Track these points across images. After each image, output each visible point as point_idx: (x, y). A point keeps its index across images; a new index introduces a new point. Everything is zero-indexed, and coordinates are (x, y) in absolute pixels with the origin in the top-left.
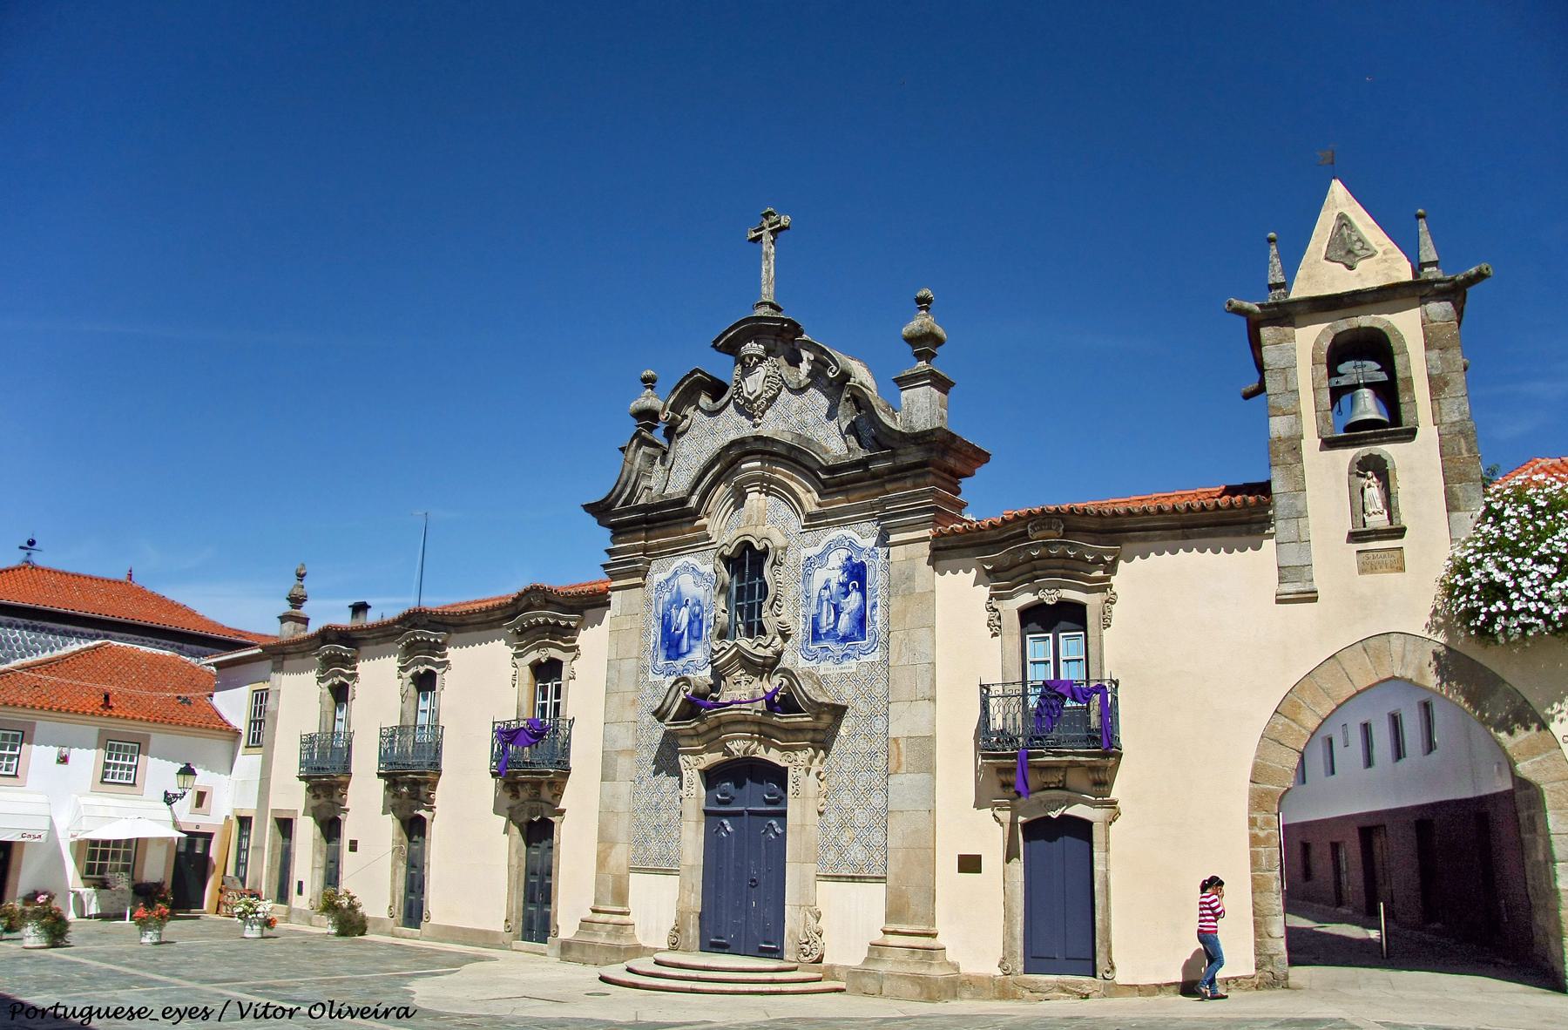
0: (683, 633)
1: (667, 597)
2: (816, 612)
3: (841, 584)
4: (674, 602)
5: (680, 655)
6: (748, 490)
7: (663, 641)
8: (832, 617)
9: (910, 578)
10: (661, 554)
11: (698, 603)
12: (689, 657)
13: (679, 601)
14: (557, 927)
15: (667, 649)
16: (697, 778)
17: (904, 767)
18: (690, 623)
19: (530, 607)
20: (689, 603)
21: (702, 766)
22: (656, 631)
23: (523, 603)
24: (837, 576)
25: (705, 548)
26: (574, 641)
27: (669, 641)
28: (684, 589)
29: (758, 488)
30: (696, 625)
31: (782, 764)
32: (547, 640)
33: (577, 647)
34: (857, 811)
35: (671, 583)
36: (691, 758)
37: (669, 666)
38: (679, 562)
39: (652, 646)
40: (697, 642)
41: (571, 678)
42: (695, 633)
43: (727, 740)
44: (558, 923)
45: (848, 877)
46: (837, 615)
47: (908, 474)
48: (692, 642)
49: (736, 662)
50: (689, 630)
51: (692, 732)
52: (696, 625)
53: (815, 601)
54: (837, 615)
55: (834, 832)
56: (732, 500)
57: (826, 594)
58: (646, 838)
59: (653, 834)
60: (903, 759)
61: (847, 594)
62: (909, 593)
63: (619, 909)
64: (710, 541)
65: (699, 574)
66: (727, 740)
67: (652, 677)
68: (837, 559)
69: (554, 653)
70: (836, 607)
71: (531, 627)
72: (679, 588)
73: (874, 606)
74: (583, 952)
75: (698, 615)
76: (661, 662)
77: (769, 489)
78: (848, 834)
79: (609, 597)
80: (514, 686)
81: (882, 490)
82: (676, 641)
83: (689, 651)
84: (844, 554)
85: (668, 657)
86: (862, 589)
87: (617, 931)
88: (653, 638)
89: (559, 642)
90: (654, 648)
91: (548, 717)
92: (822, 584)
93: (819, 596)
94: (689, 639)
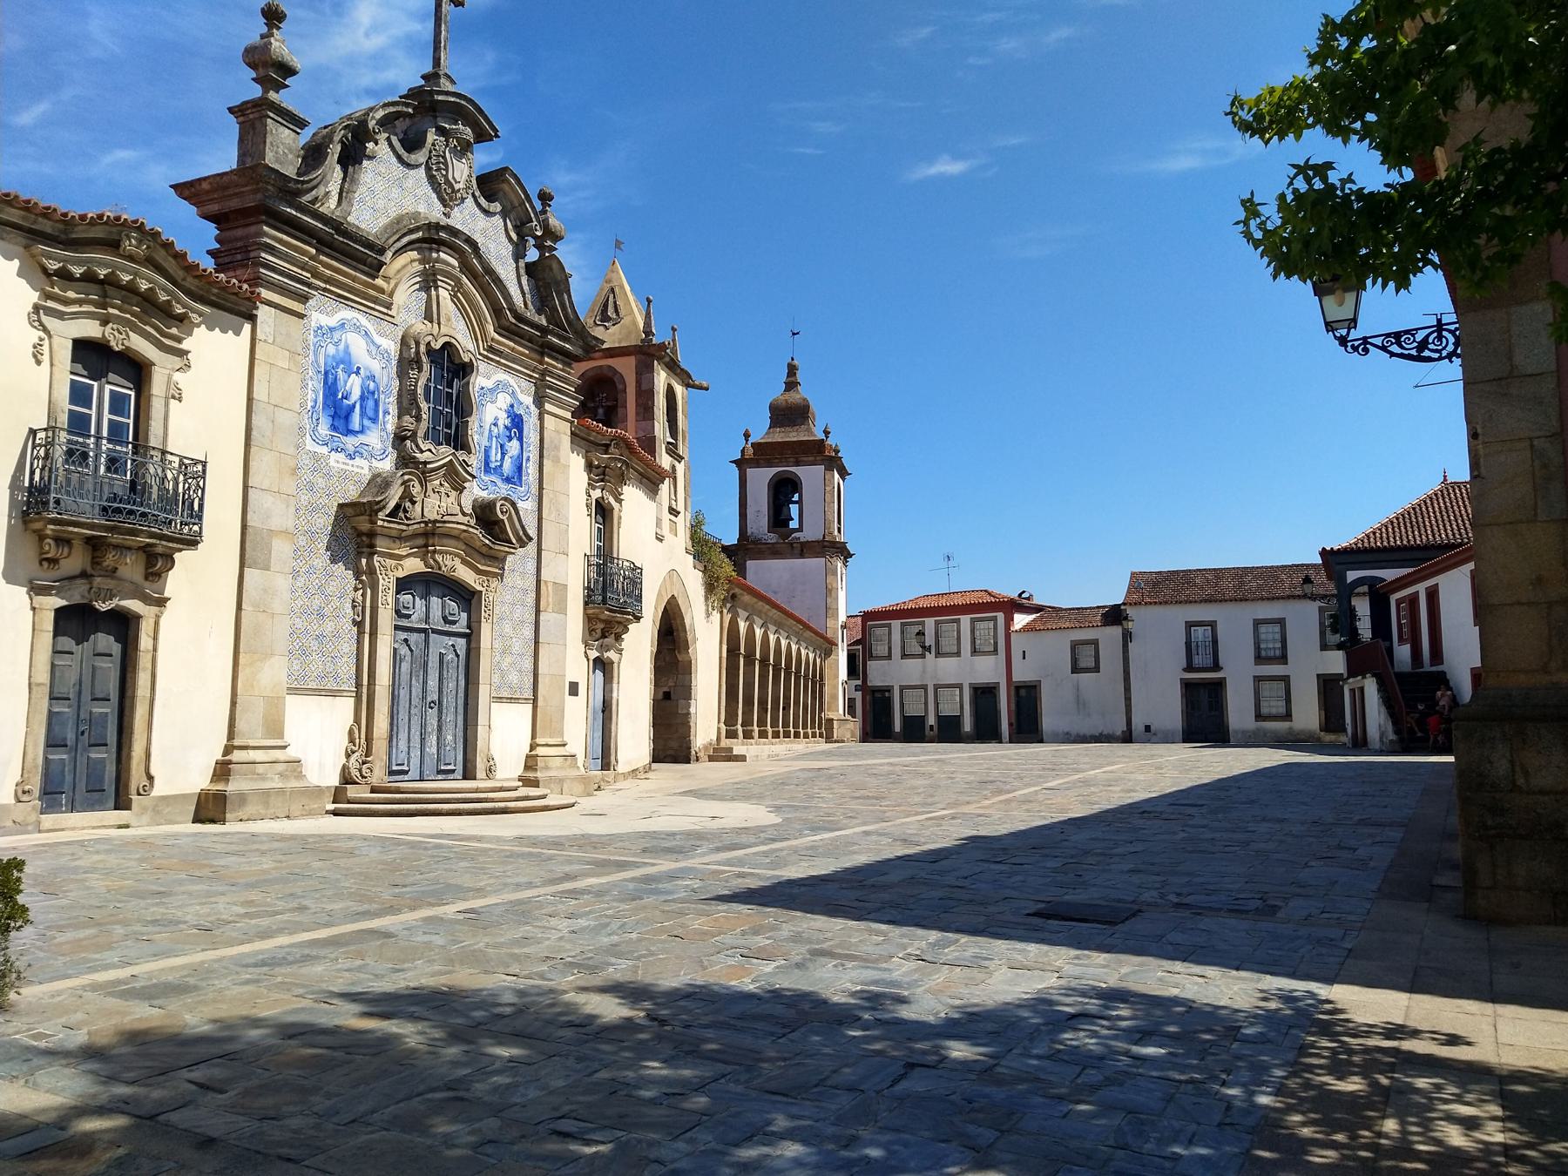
0: (354, 406)
1: (331, 350)
2: (487, 444)
3: (506, 427)
4: (342, 362)
5: (349, 432)
6: (440, 283)
7: (324, 403)
8: (499, 455)
9: (557, 448)
10: (325, 290)
11: (372, 378)
12: (362, 438)
13: (346, 362)
14: (150, 778)
15: (333, 417)
16: (393, 586)
17: (551, 606)
18: (363, 398)
19: (113, 245)
20: (362, 371)
21: (401, 574)
22: (314, 390)
23: (98, 233)
24: (504, 420)
25: (382, 316)
26: (179, 340)
27: (335, 408)
28: (353, 350)
29: (450, 288)
30: (370, 403)
31: (479, 588)
32: (128, 316)
33: (187, 352)
34: (514, 640)
35: (336, 335)
36: (390, 562)
37: (336, 439)
38: (347, 314)
39: (310, 404)
40: (372, 425)
41: (173, 397)
42: (370, 413)
43: (441, 552)
44: (153, 772)
45: (507, 698)
46: (503, 455)
47: (560, 357)
48: (366, 422)
49: (442, 471)
50: (361, 406)
51: (394, 533)
52: (370, 403)
53: (486, 433)
54: (503, 455)
55: (498, 658)
56: (418, 279)
57: (495, 430)
58: (304, 652)
59: (314, 645)
60: (550, 600)
61: (510, 439)
62: (557, 460)
63: (279, 743)
64: (390, 313)
65: (373, 342)
66: (441, 552)
67: (310, 445)
68: (503, 400)
69: (140, 345)
70: (502, 446)
71: (110, 282)
72: (347, 347)
73: (528, 459)
74: (266, 804)
75: (373, 393)
76: (324, 430)
77: (455, 293)
78: (508, 660)
79: (257, 308)
80: (39, 363)
81: (538, 357)
82: (343, 414)
83: (362, 432)
84: (509, 400)
85: (334, 428)
86: (520, 439)
87: (295, 770)
88: (311, 396)
89: (148, 328)
90: (313, 407)
91: (93, 432)
92: (492, 420)
93: (490, 431)
94: (363, 414)
